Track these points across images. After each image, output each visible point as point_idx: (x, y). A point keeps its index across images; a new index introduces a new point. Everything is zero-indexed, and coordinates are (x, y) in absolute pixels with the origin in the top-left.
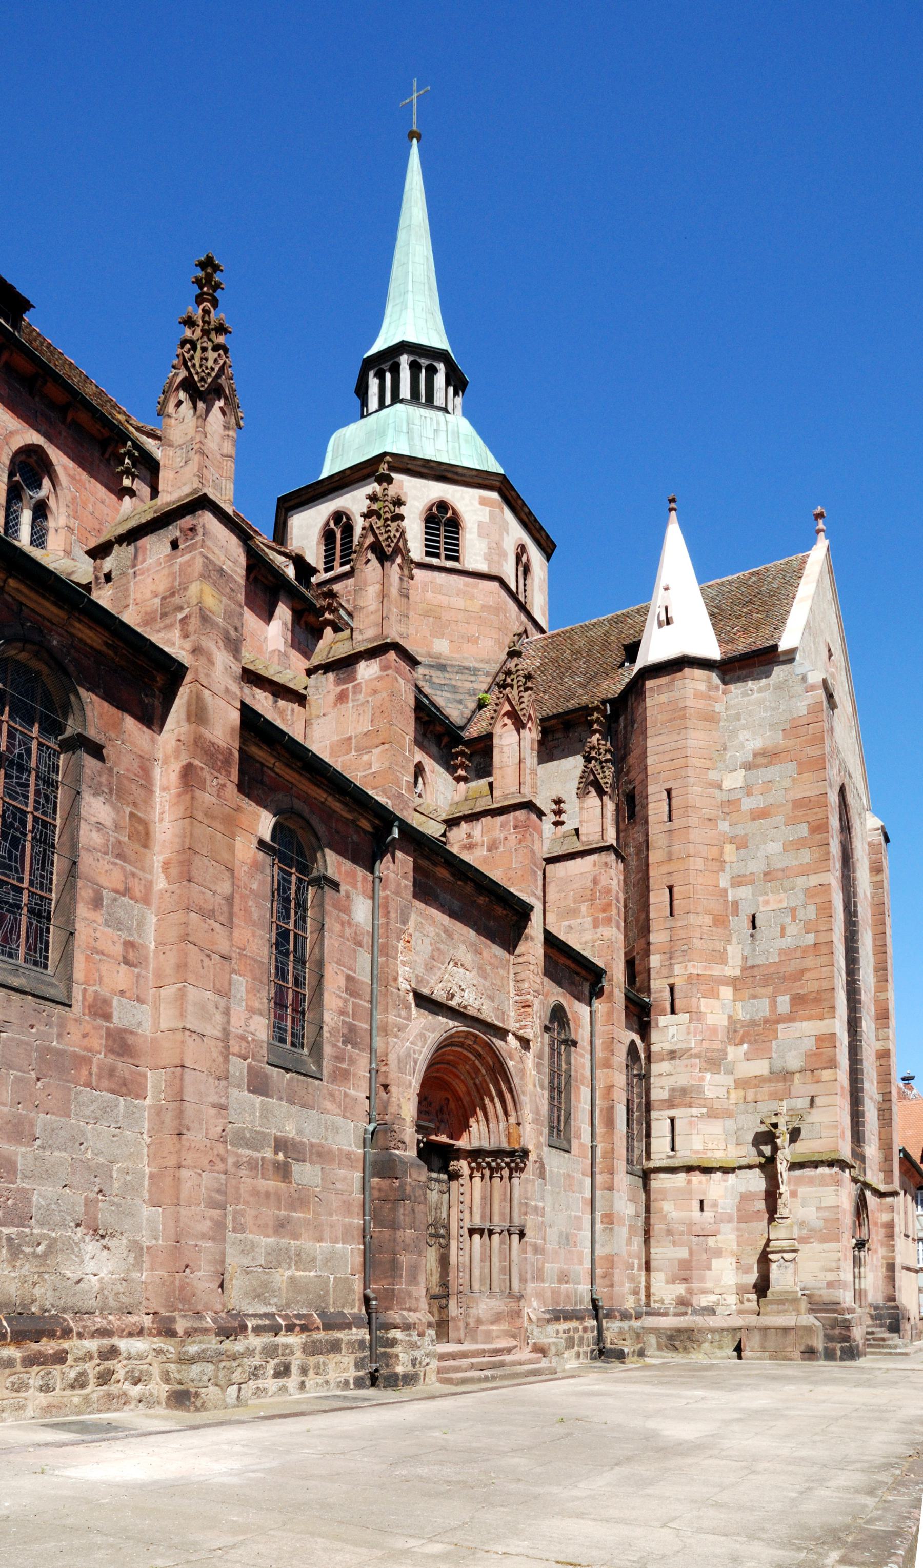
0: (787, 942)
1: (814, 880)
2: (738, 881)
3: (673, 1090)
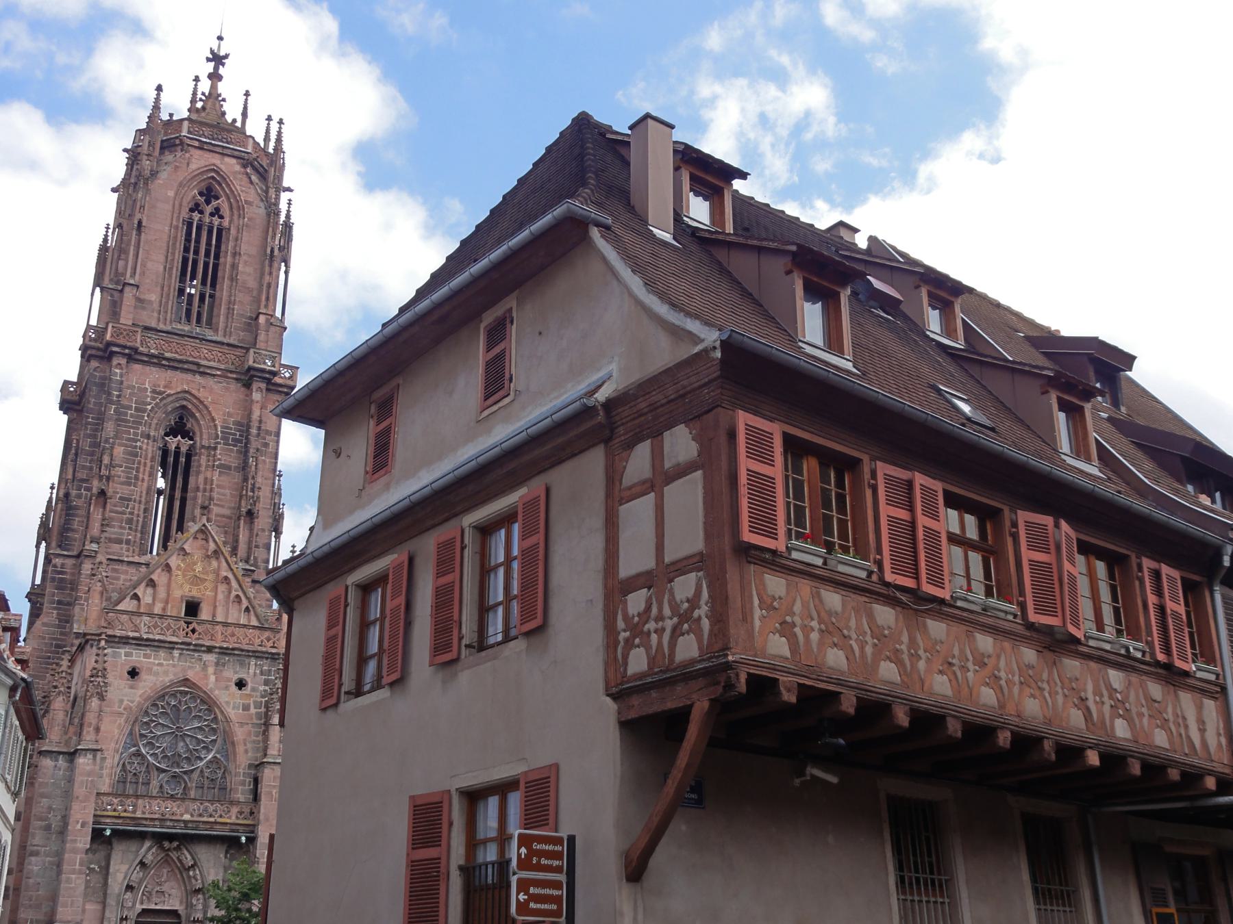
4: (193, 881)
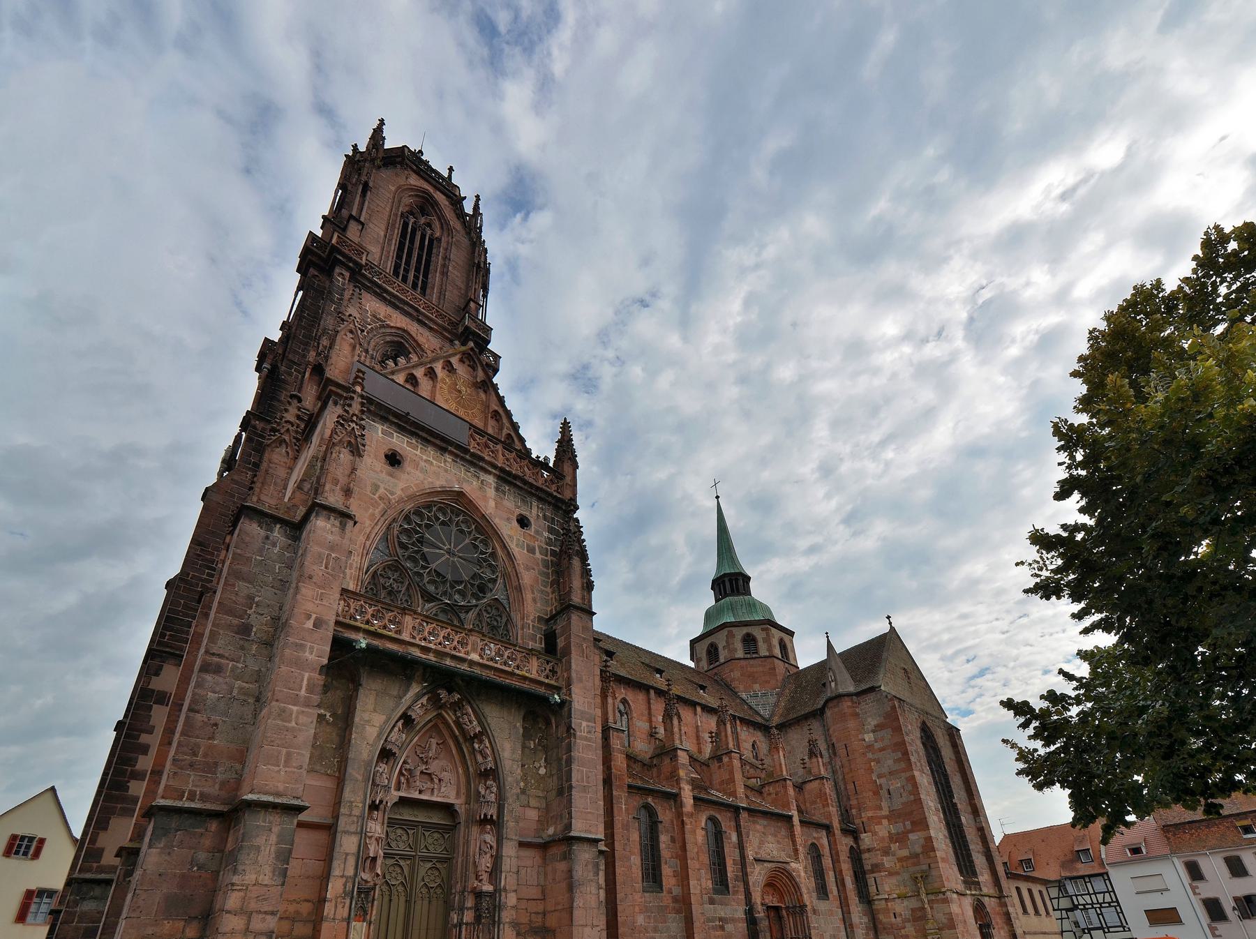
0: (904, 799)
1: (908, 774)
2: (880, 776)
3: (872, 865)
4: (480, 758)
